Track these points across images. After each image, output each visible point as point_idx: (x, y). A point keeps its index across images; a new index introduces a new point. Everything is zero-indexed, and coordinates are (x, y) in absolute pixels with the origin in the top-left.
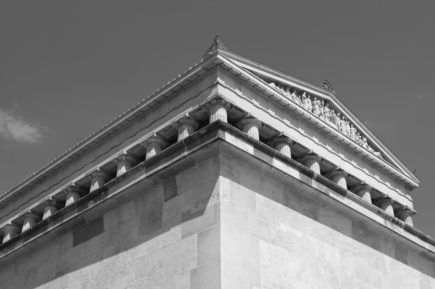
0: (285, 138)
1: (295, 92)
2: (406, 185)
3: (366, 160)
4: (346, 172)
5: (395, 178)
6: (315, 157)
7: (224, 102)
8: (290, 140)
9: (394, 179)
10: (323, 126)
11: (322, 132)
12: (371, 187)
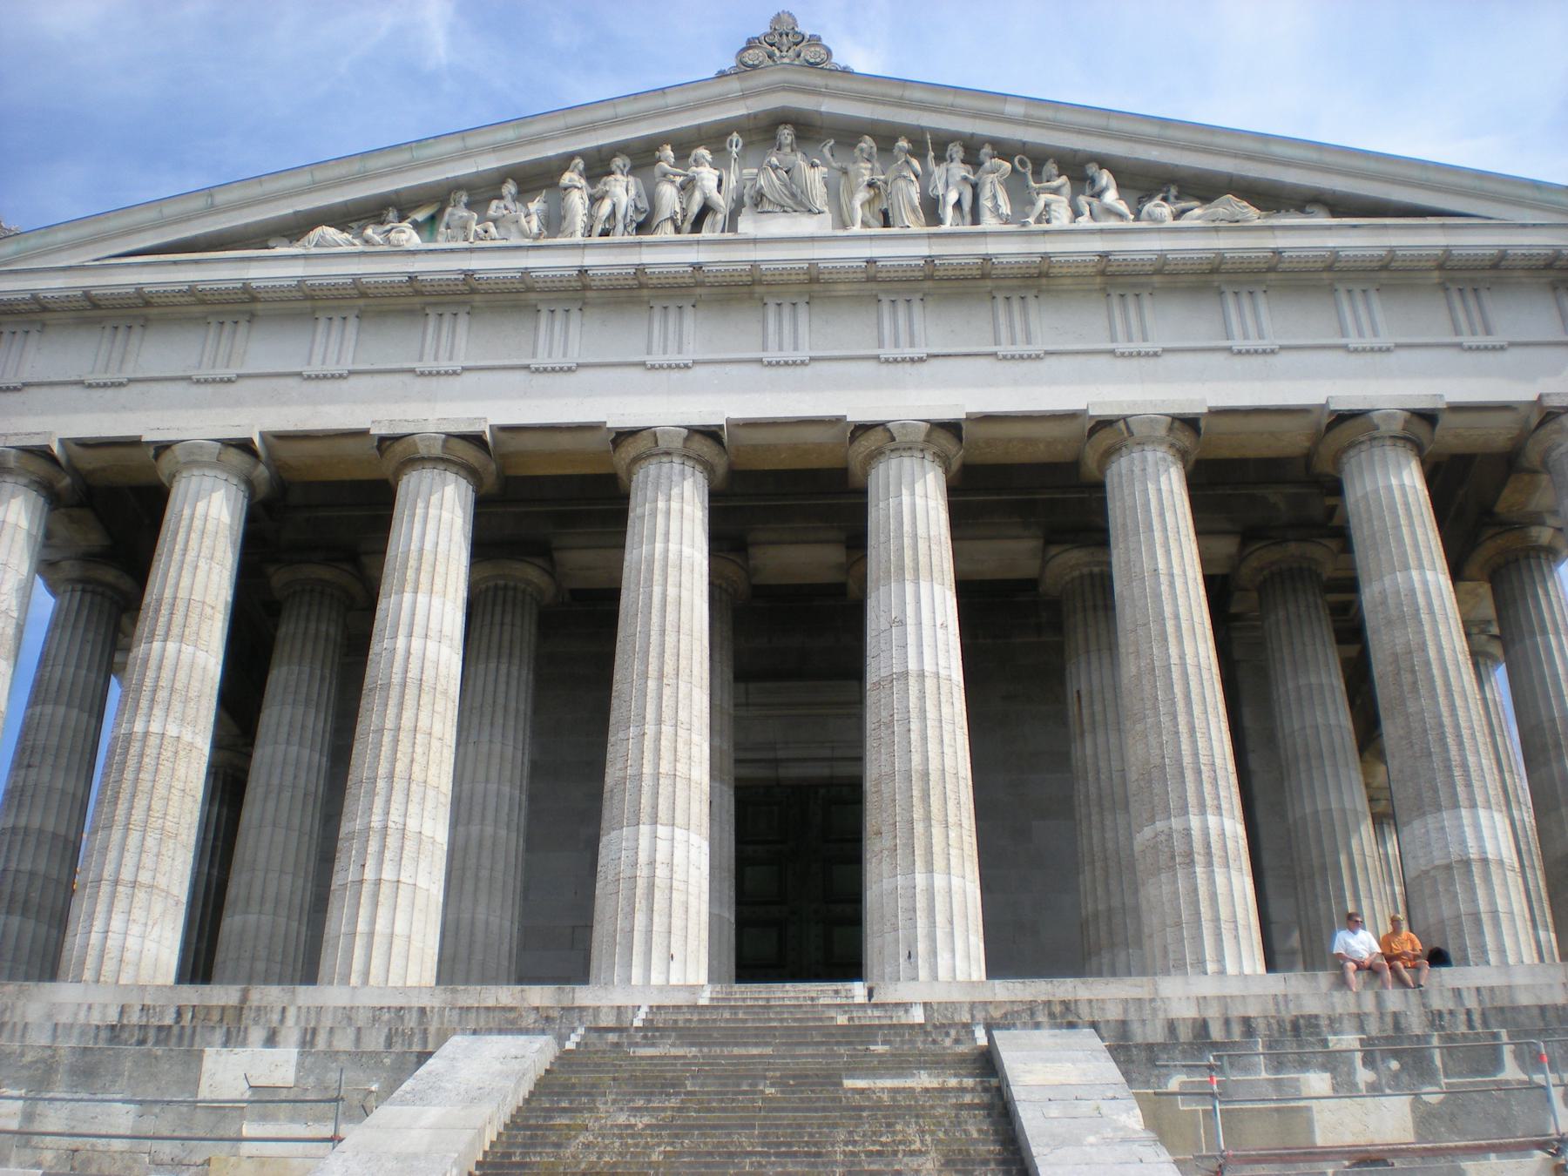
0: (399, 447)
1: (510, 188)
2: (1552, 273)
3: (1134, 280)
5: (1436, 274)
6: (641, 445)
8: (428, 438)
9: (1436, 281)
10: (691, 265)
11: (726, 290)
12: (1152, 420)
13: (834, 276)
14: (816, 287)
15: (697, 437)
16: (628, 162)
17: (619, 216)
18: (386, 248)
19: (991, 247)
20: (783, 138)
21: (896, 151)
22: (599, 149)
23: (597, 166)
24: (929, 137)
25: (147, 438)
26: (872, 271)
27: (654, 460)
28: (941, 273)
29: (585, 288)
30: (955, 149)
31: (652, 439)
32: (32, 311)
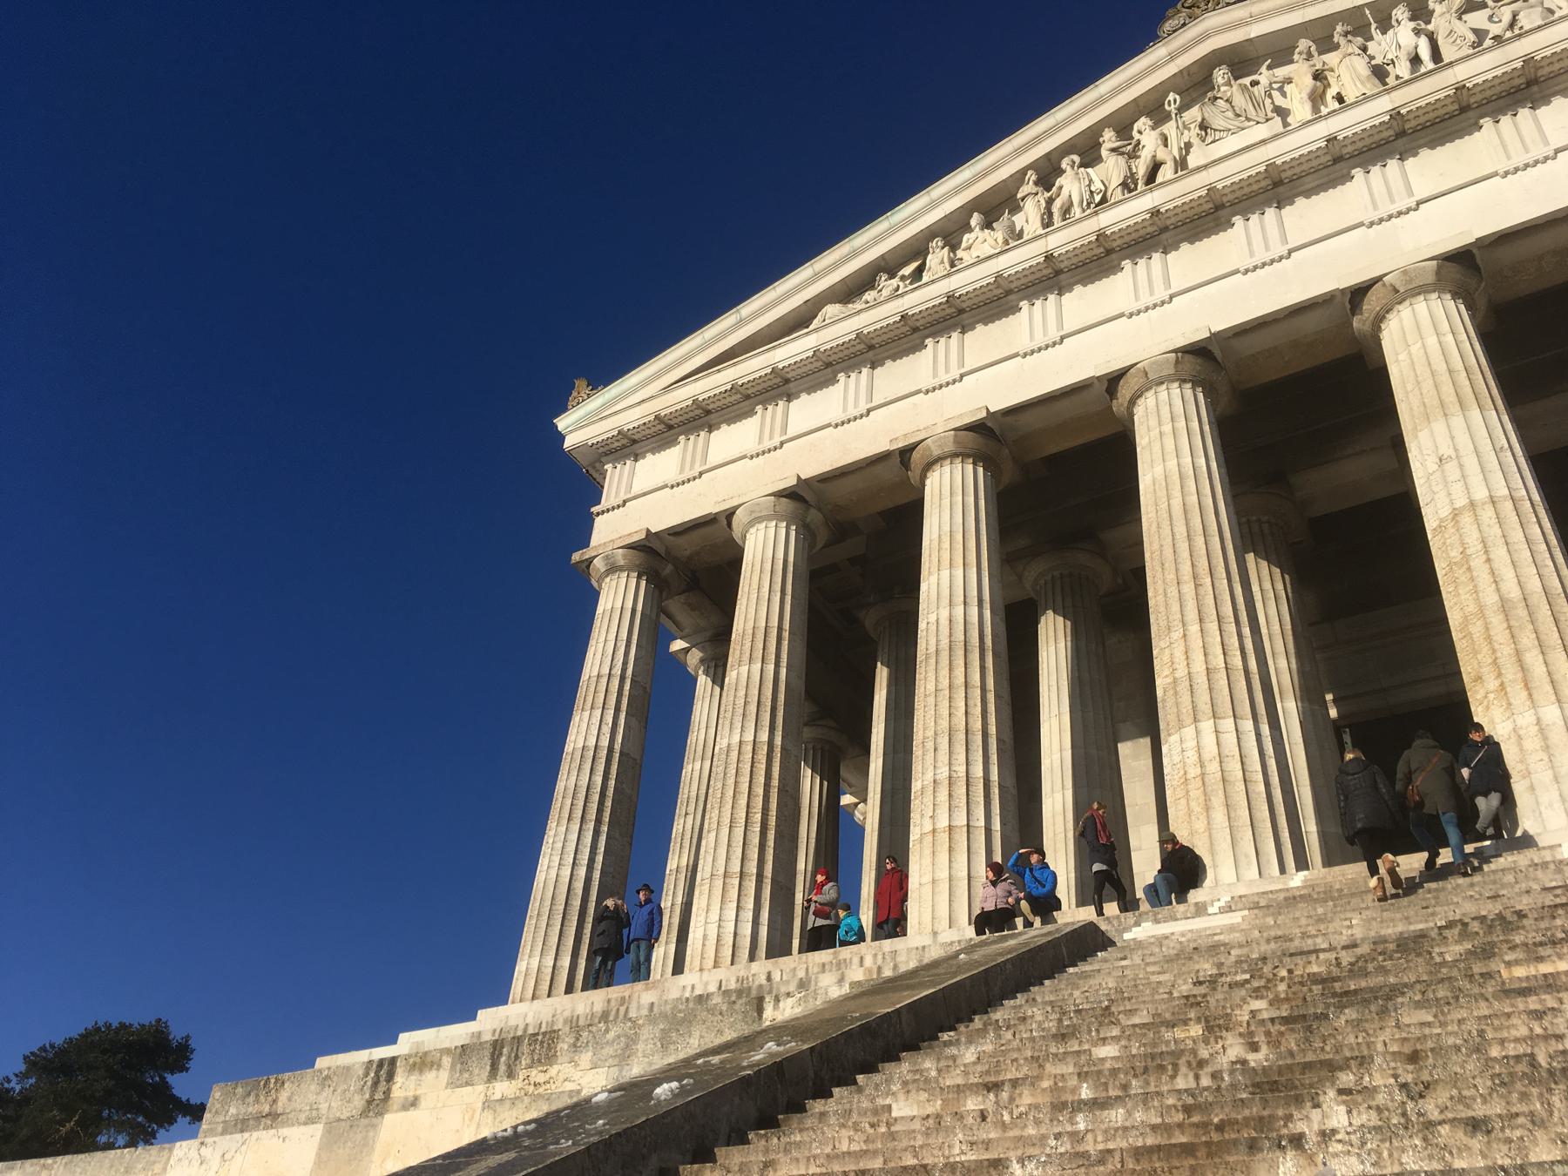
0: (916, 455)
1: (975, 219)
4: (1405, 272)
7: (603, 564)
13: (1297, 170)
14: (1281, 189)
15: (1188, 357)
16: (1076, 158)
17: (1076, 200)
18: (882, 299)
19: (1460, 73)
20: (1220, 81)
21: (1336, 40)
22: (1048, 156)
23: (1048, 173)
24: (1367, 12)
25: (715, 510)
26: (1336, 150)
27: (1150, 394)
28: (1413, 123)
29: (1058, 272)
30: (1399, 12)
31: (1142, 374)
32: (624, 447)
